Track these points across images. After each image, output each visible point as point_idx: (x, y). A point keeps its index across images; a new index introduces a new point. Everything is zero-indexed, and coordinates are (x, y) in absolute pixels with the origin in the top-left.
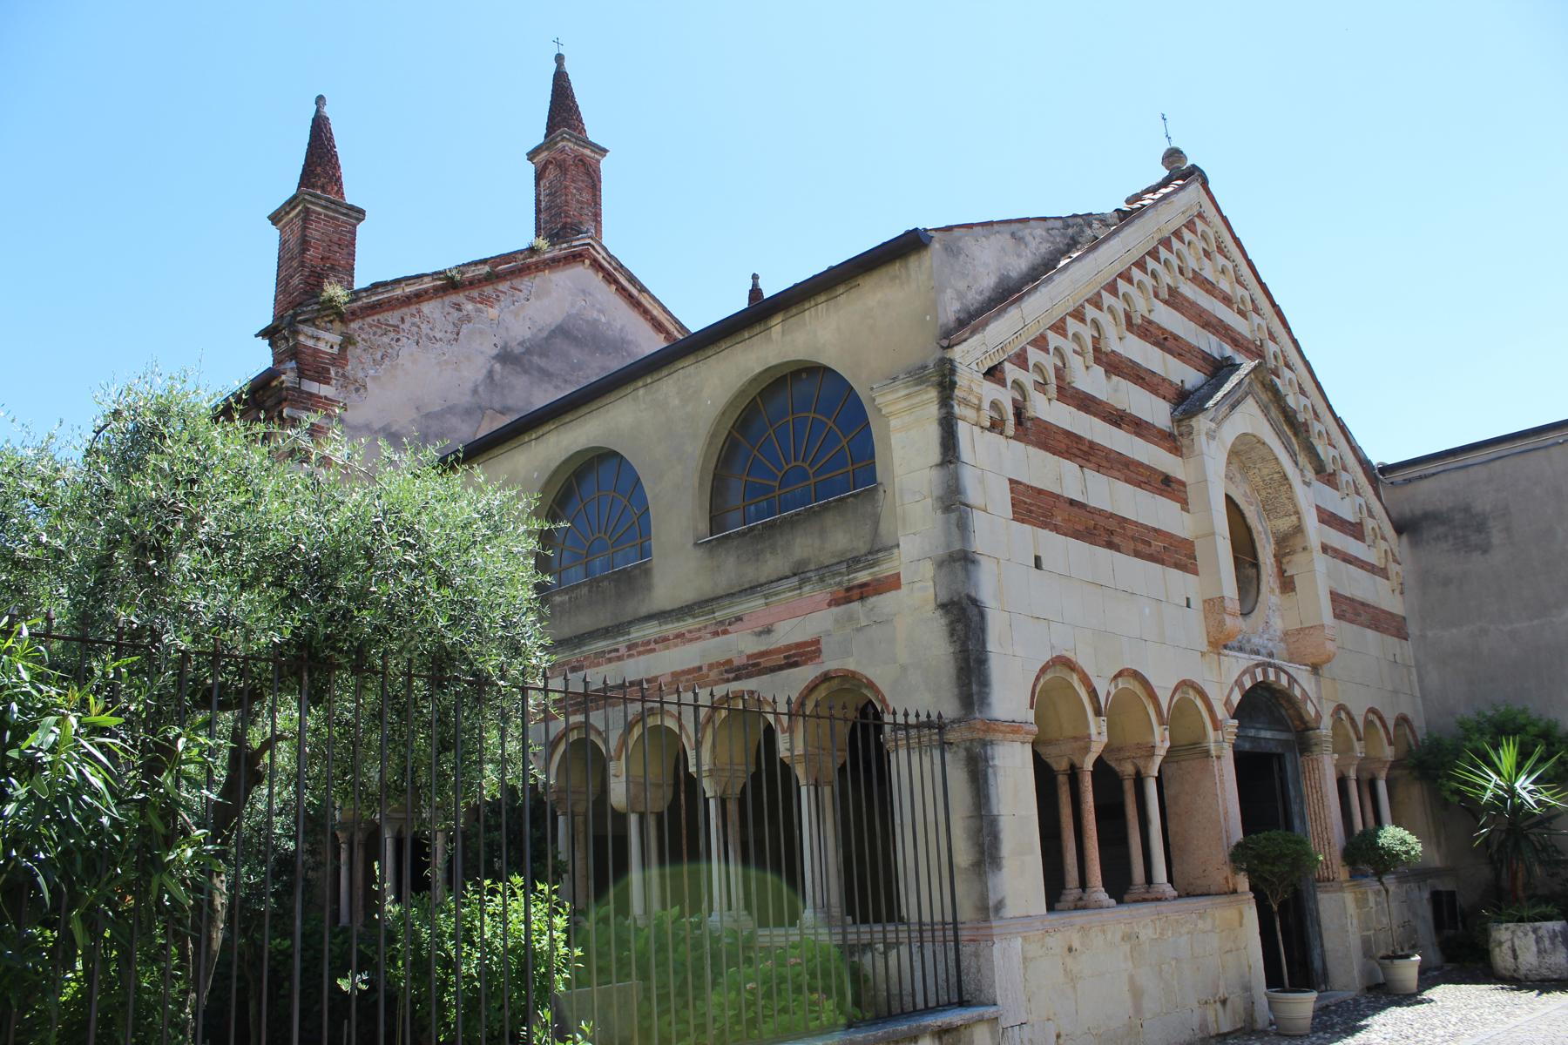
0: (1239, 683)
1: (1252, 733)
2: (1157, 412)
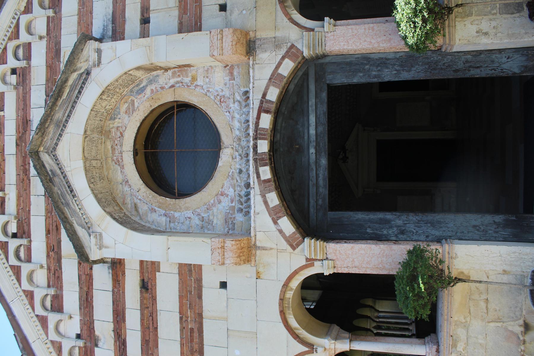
1: (312, 151)
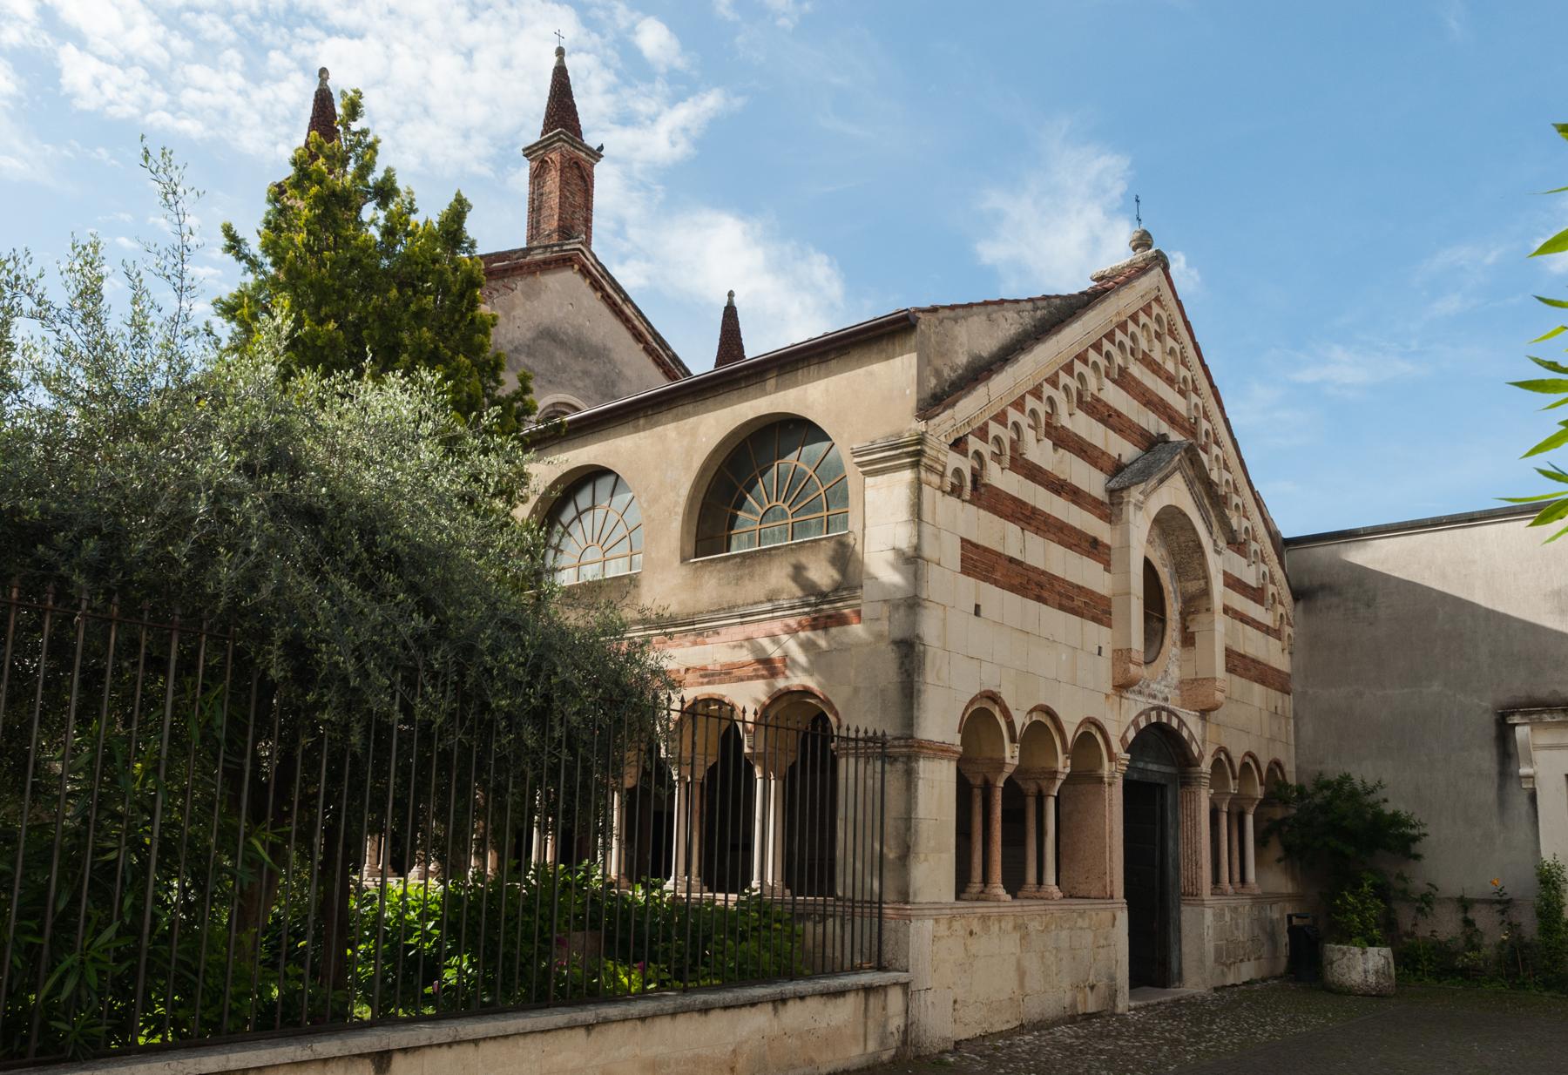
0: (1135, 723)
1: (1141, 765)
2: (1092, 481)
